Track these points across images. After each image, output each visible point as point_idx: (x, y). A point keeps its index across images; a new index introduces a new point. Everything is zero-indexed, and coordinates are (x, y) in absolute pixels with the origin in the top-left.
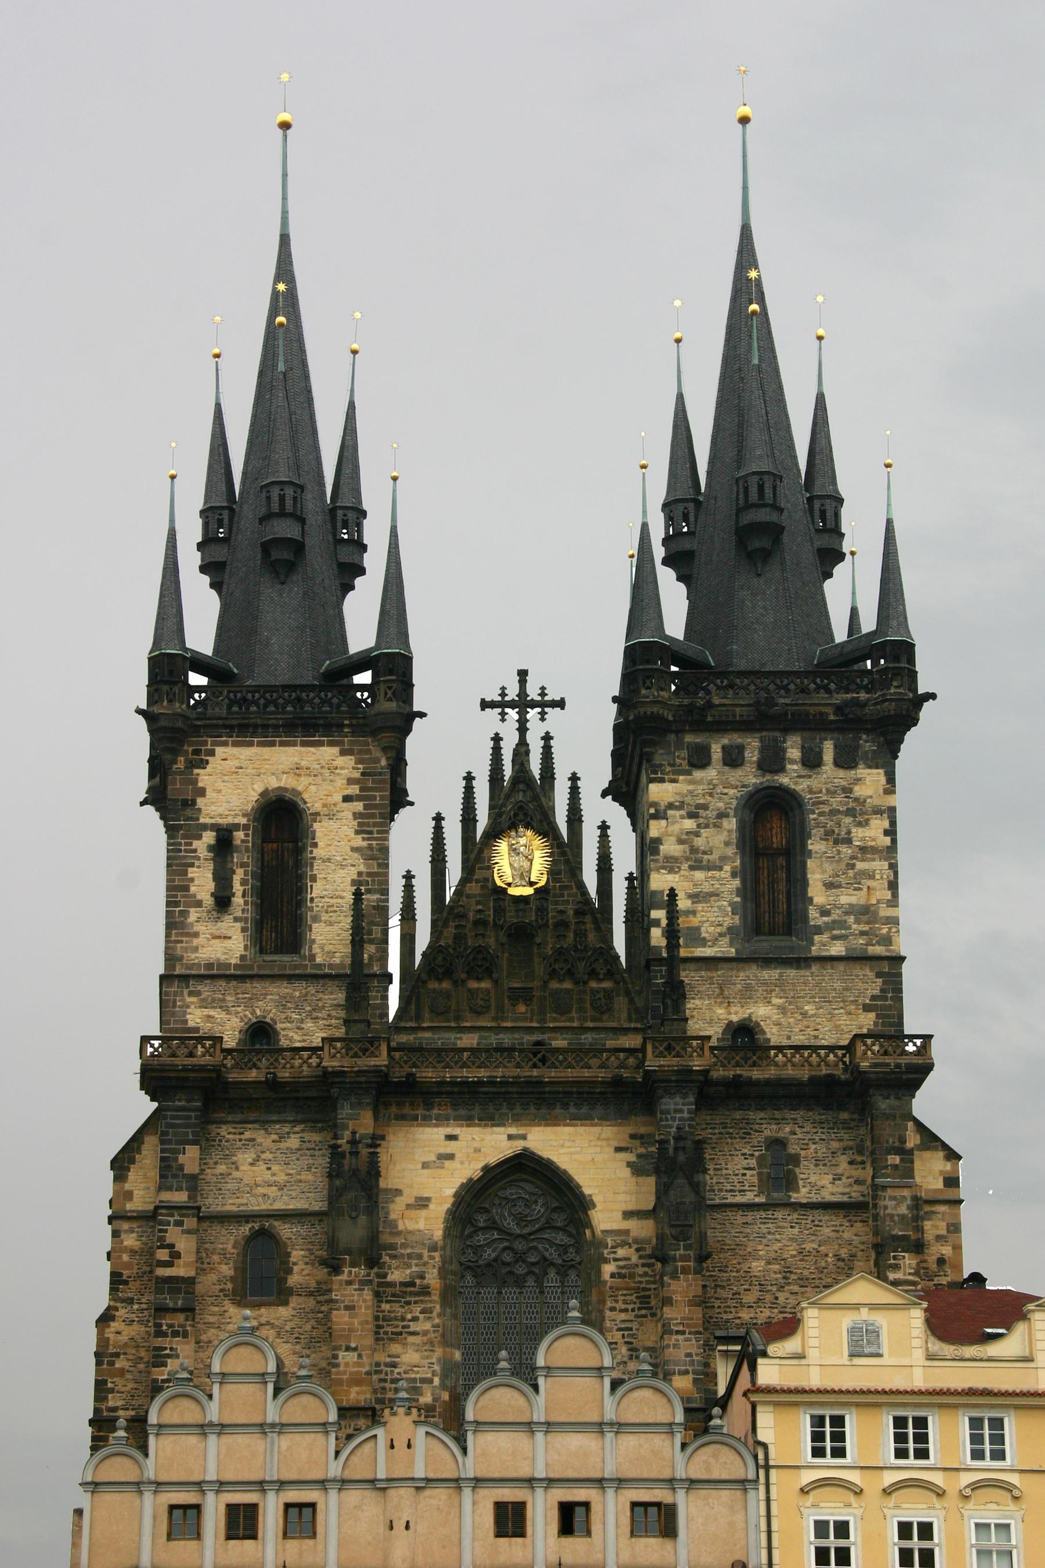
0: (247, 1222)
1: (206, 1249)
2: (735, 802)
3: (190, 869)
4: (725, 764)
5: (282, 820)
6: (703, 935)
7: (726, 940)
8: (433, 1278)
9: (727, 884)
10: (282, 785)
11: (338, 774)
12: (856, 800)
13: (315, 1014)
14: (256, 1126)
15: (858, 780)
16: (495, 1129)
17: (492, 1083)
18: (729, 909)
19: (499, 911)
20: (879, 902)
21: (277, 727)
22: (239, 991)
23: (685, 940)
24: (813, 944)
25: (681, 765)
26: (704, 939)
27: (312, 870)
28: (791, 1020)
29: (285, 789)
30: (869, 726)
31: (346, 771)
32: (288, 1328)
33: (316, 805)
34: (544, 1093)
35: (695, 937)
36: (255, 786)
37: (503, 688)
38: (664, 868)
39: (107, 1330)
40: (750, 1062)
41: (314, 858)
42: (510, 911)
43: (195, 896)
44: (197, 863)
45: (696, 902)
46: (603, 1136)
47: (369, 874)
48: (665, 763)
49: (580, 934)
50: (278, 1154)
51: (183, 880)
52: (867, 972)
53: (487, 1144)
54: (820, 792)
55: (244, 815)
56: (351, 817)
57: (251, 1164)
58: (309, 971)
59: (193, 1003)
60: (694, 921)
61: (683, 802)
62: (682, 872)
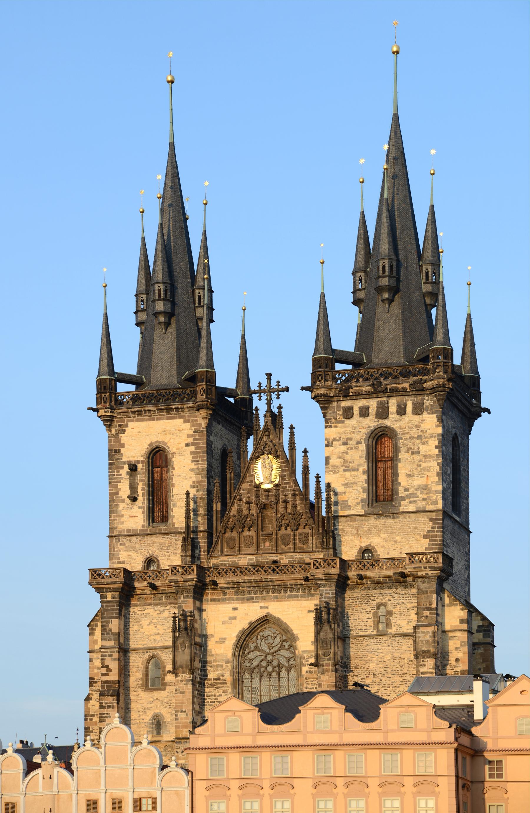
0: (147, 652)
2: (365, 436)
7: (360, 506)
8: (228, 676)
9: (360, 478)
10: (158, 440)
12: (422, 431)
13: (175, 552)
14: (150, 607)
16: (255, 604)
18: (362, 490)
19: (257, 497)
20: (432, 483)
22: (142, 542)
24: (400, 506)
26: (350, 506)
28: (390, 545)
29: (160, 442)
31: (186, 431)
32: (165, 701)
38: (331, 471)
39: (89, 705)
41: (173, 475)
42: (262, 497)
43: (121, 497)
44: (122, 481)
45: (346, 488)
47: (198, 482)
49: (294, 506)
50: (159, 620)
52: (425, 518)
54: (405, 428)
55: (142, 456)
56: (189, 453)
59: (122, 549)
62: (340, 473)
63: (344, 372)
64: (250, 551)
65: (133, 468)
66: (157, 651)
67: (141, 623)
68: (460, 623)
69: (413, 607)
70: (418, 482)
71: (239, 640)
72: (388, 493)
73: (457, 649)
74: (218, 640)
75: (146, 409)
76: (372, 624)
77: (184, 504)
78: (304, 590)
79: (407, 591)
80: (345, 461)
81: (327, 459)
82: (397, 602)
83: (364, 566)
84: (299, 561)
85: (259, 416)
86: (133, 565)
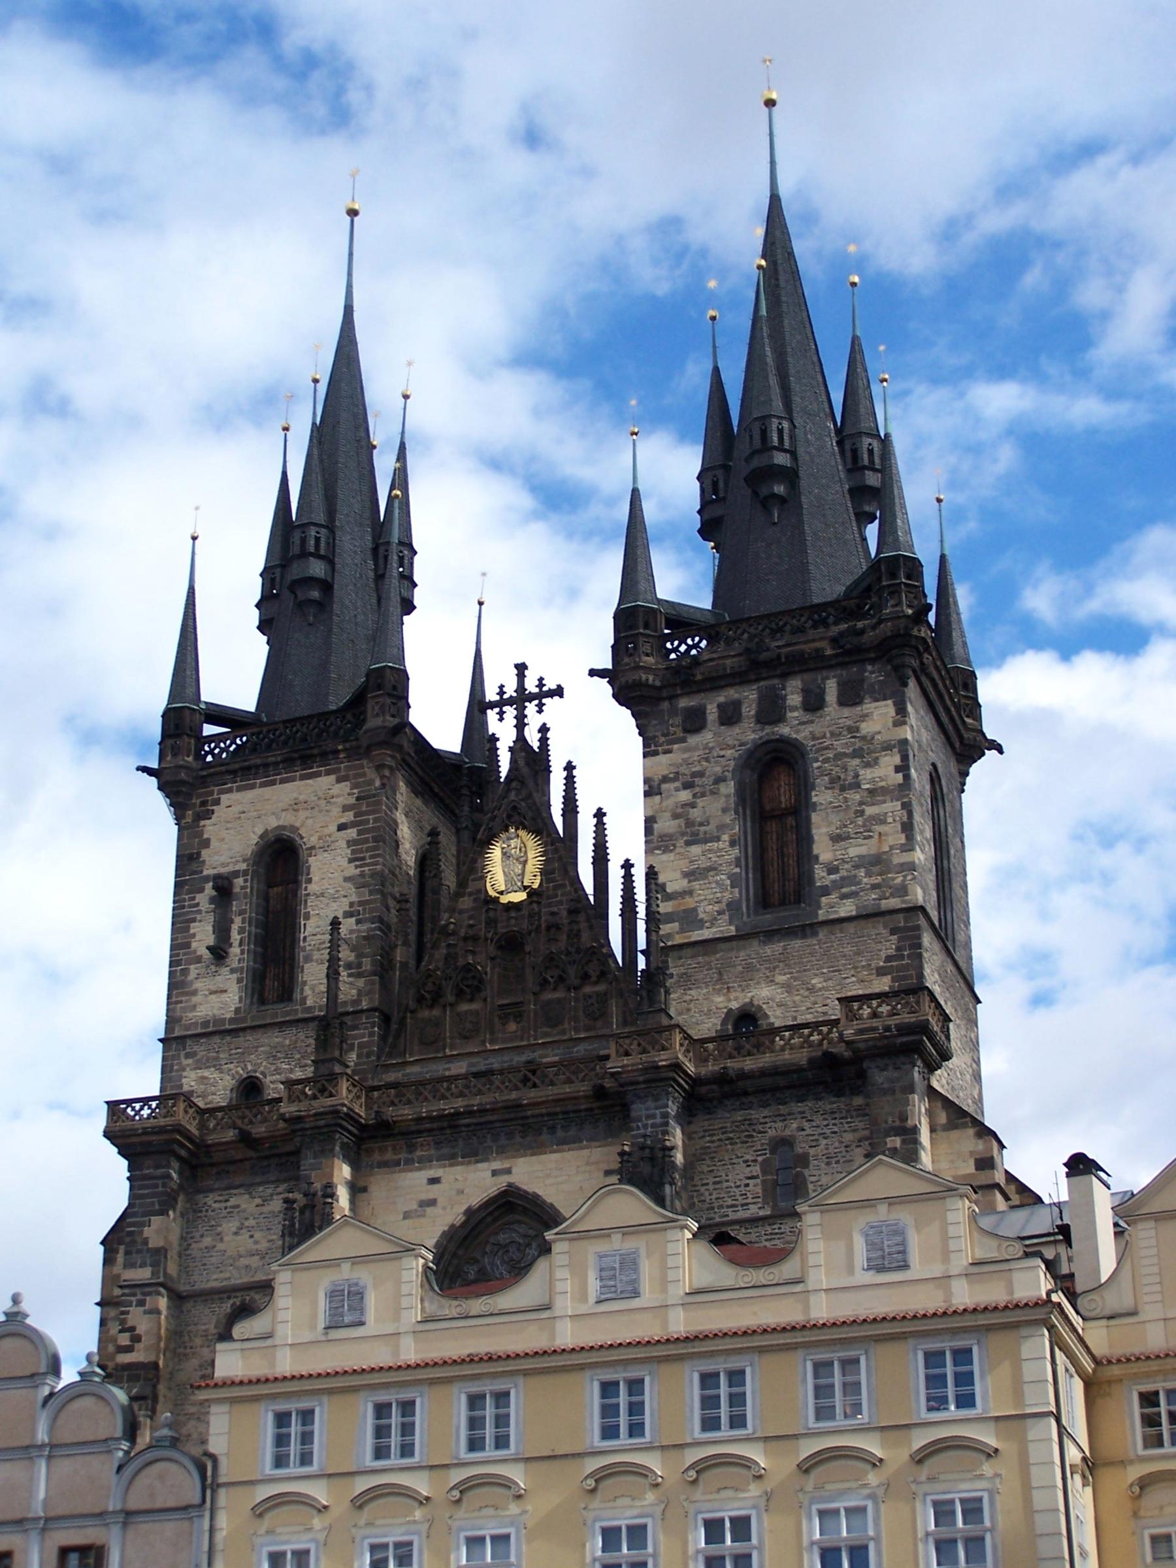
0: (229, 1298)
1: (189, 1332)
2: (732, 763)
3: (192, 925)
4: (722, 724)
5: (281, 858)
6: (701, 916)
7: (726, 917)
9: (725, 854)
11: (335, 803)
12: (863, 738)
13: (304, 1062)
15: (864, 717)
16: (480, 1165)
17: (470, 1113)
18: (728, 882)
19: (491, 923)
20: (892, 848)
21: (276, 764)
22: (232, 1046)
23: (681, 925)
24: (820, 908)
25: (675, 733)
26: (701, 920)
27: (306, 908)
28: (797, 998)
29: (283, 828)
30: (872, 655)
33: (312, 839)
34: (527, 1118)
35: (689, 919)
36: (256, 829)
37: (501, 687)
38: (658, 848)
40: (744, 1052)
41: (308, 895)
43: (195, 952)
44: (199, 917)
47: (361, 903)
48: (659, 734)
51: (185, 937)
52: (879, 929)
53: (470, 1184)
54: (824, 736)
55: (244, 861)
57: (236, 1234)
58: (300, 1016)
60: (689, 902)
61: (677, 773)
62: (677, 850)
65: (224, 889)
66: (252, 1293)
67: (219, 1229)
68: (977, 1169)
69: (860, 1141)
70: (856, 850)
75: (259, 761)
76: (759, 1190)
79: (841, 1103)
81: (649, 822)
85: (499, 752)
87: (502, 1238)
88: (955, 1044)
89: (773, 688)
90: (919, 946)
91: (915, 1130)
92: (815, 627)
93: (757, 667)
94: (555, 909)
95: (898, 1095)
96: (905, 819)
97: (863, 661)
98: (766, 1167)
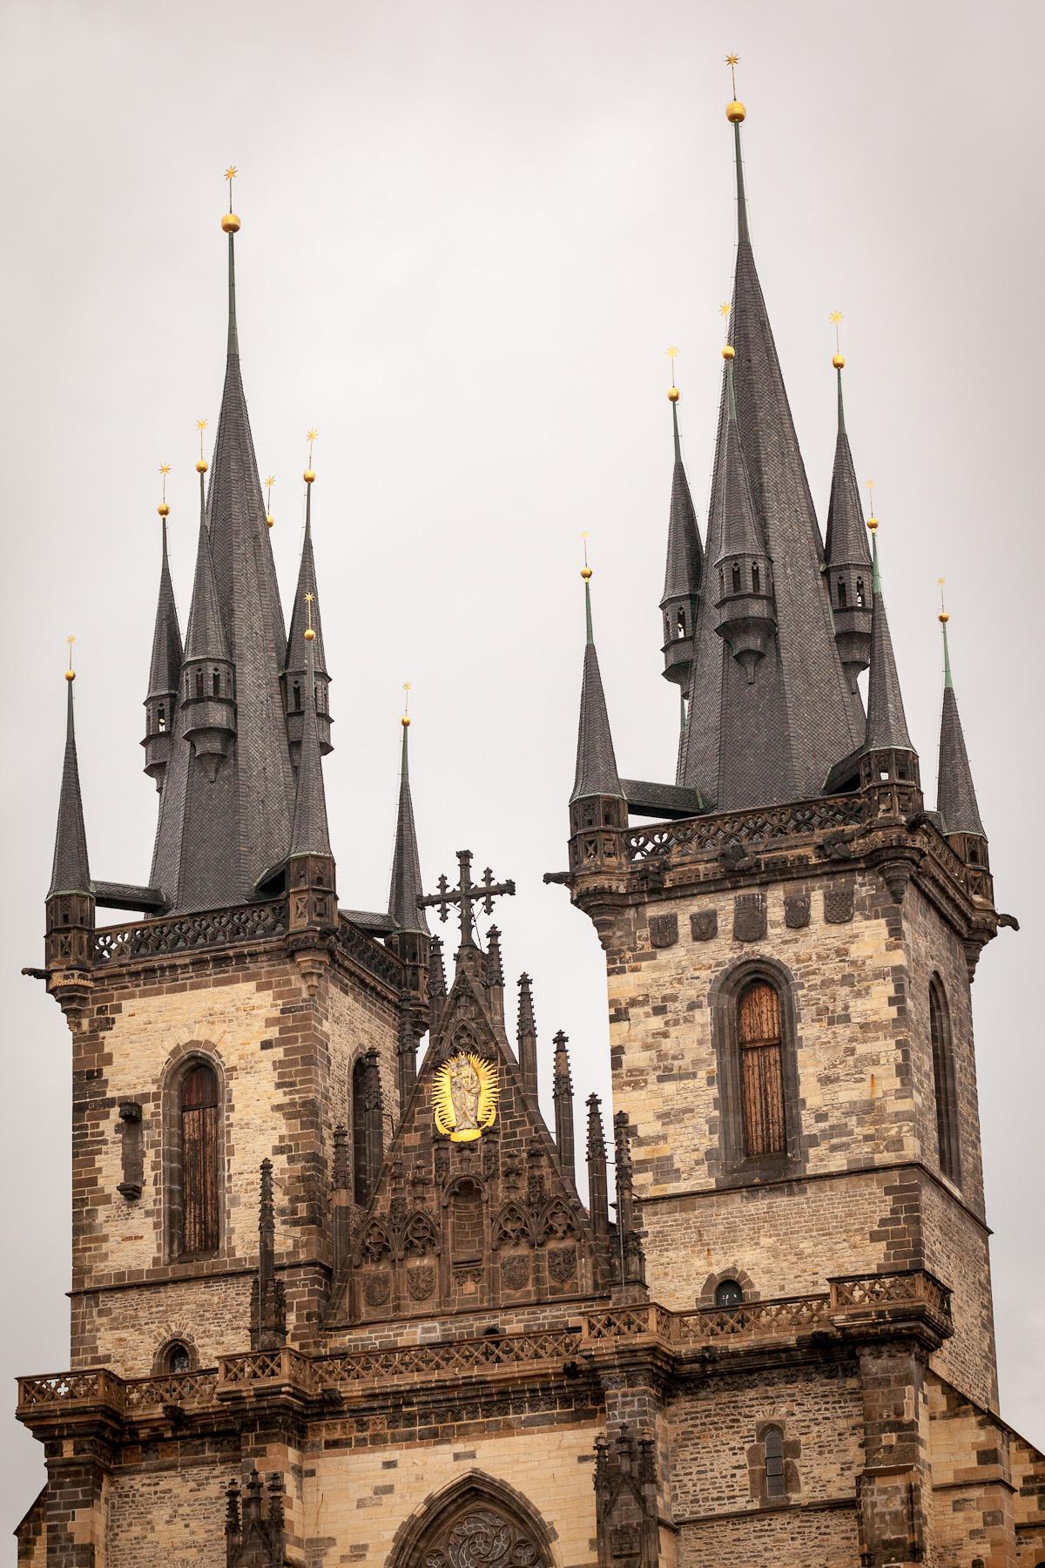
2: (708, 986)
4: (696, 939)
5: (197, 1077)
7: (705, 1167)
9: (702, 1095)
10: (195, 1038)
12: (853, 963)
13: (235, 1324)
14: (173, 1473)
16: (439, 1447)
20: (885, 1094)
21: (186, 966)
26: (678, 1170)
28: (785, 1264)
29: (198, 1043)
35: (665, 1169)
37: (443, 878)
38: (628, 1083)
41: (231, 1125)
43: (102, 1189)
46: (565, 1443)
47: (292, 1137)
49: (535, 1182)
52: (872, 1188)
55: (154, 1082)
60: (664, 1149)
62: (650, 1087)
63: (649, 832)
64: (428, 1307)
65: (132, 1118)
70: (849, 1093)
71: (403, 1548)
72: (775, 1130)
73: (974, 1533)
74: (346, 1551)
76: (747, 1481)
77: (256, 1197)
78: (566, 1402)
79: (834, 1386)
80: (662, 1056)
81: (617, 1052)
82: (811, 1415)
83: (721, 1324)
84: (551, 1324)
85: (443, 959)
86: (130, 1364)
87: (468, 1528)
88: (959, 1322)
89: (752, 899)
90: (917, 1209)
91: (913, 1425)
92: (797, 829)
93: (733, 874)
94: (513, 1151)
95: (893, 1387)
96: (900, 1060)
97: (853, 870)
98: (753, 1455)
